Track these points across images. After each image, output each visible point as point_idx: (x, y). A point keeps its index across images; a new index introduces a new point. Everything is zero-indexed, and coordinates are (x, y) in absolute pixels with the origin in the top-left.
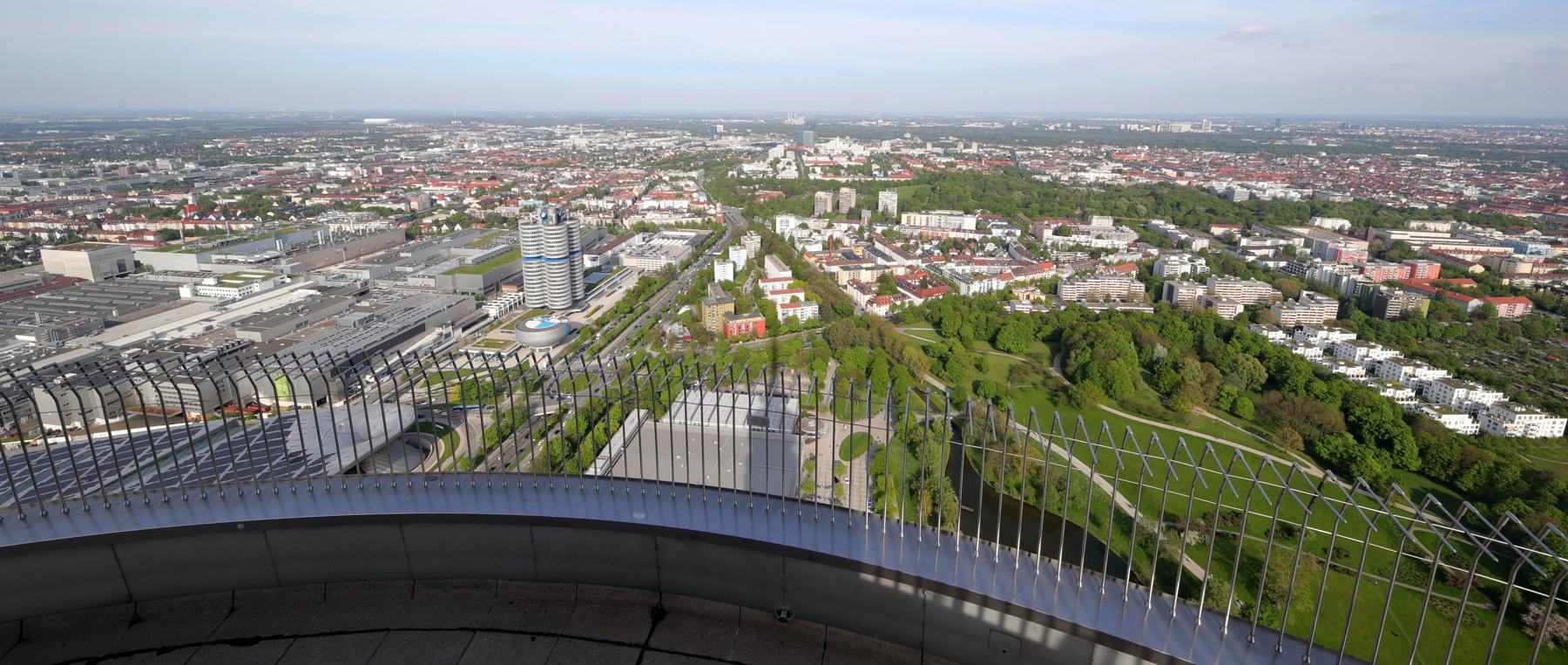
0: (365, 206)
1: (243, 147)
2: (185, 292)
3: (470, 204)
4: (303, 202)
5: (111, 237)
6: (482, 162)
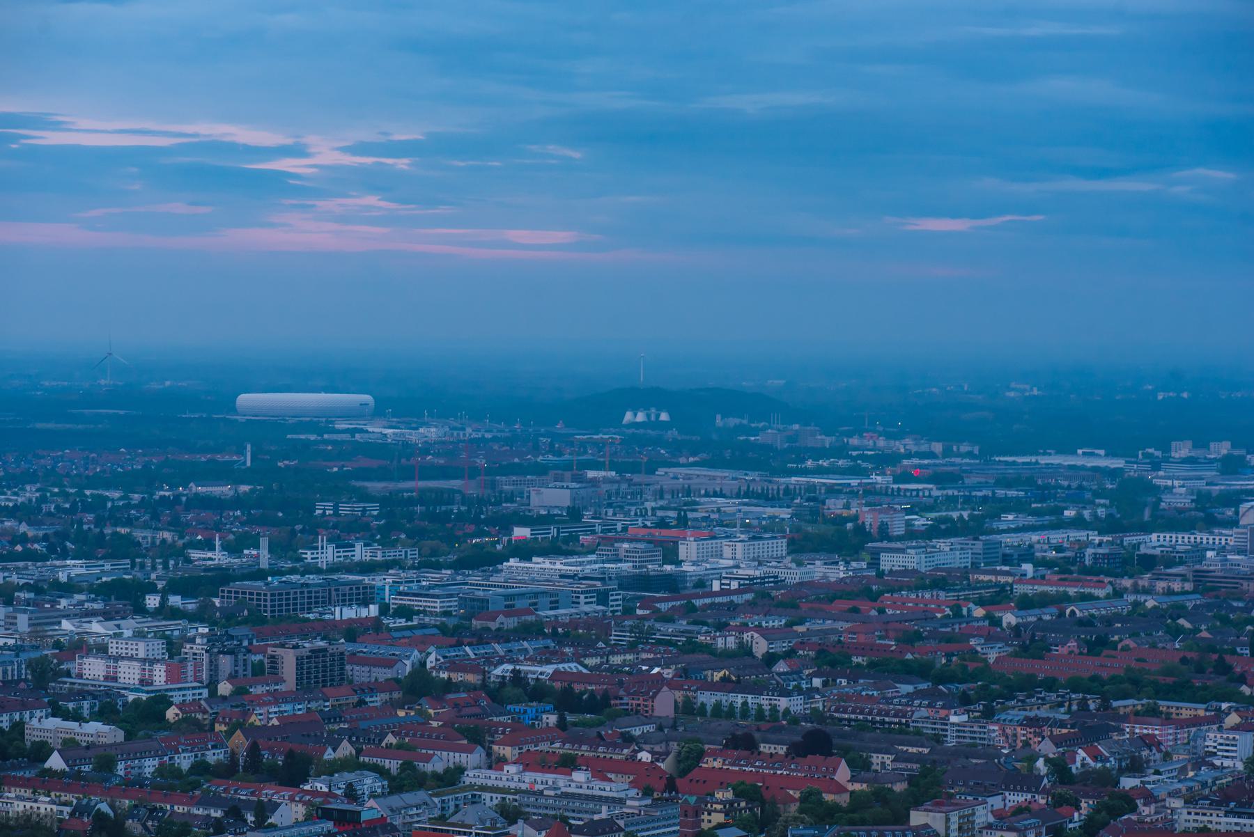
6: (761, 647)
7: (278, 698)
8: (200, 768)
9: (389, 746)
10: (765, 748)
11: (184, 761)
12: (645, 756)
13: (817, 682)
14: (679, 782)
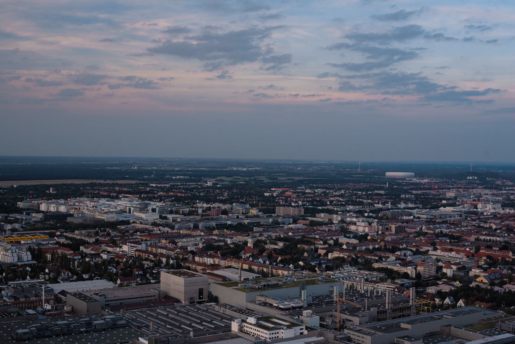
0: (376, 265)
1: (290, 197)
2: (235, 327)
3: (477, 276)
4: (326, 254)
5: (199, 268)
6: (494, 227)
7: (391, 235)
8: (374, 249)
9: (414, 245)
10: (494, 248)
11: (371, 247)
12: (468, 249)
13: (506, 235)
14: (475, 255)
